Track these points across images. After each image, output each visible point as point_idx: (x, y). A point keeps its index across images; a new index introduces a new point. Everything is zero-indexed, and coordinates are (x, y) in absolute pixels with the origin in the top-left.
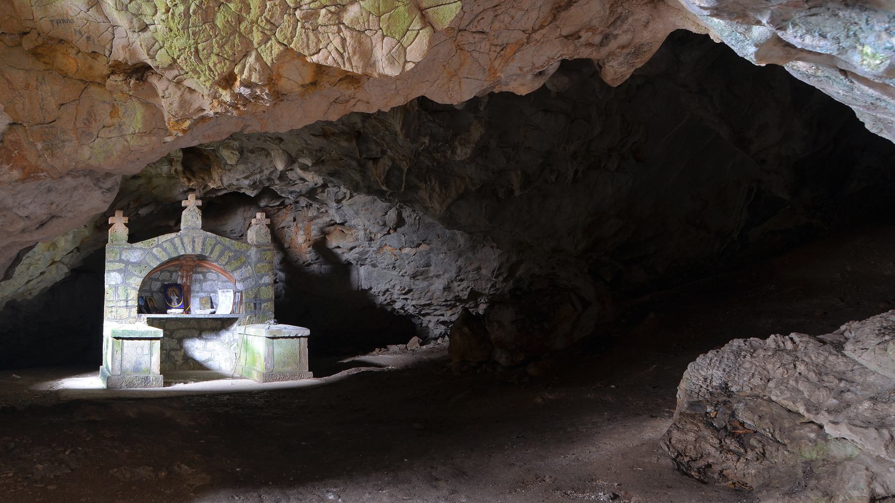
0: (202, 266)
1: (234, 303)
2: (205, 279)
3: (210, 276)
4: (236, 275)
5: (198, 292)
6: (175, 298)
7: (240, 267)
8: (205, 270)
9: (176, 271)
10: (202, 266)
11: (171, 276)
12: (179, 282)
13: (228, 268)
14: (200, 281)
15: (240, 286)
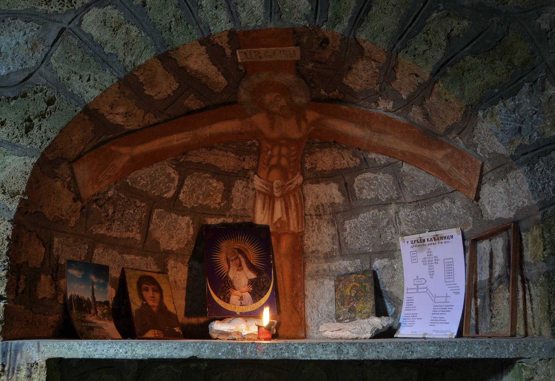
0: (336, 141)
1: (472, 290)
2: (351, 205)
3: (372, 185)
4: (490, 135)
5: (329, 257)
6: (242, 278)
7: (507, 91)
8: (346, 160)
9: (244, 175)
10: (336, 141)
11: (227, 195)
12: (261, 218)
13: (446, 104)
14: (337, 215)
15: (501, 200)
